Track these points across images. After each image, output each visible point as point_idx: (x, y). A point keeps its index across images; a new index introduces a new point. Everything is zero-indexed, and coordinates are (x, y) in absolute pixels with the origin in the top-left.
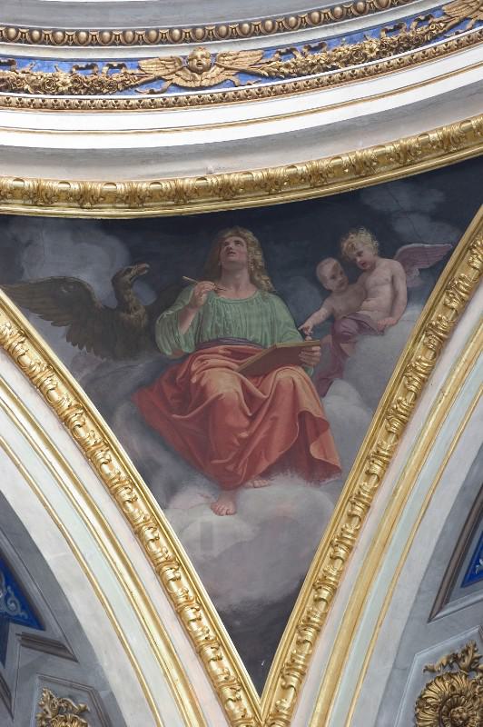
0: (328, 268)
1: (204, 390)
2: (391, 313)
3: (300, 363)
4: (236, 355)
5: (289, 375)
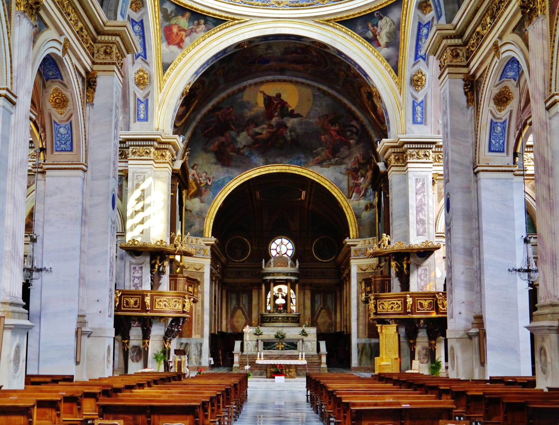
0: (196, 22)
1: (172, 30)
2: (200, 31)
3: (185, 32)
4: (179, 27)
5: (183, 33)
